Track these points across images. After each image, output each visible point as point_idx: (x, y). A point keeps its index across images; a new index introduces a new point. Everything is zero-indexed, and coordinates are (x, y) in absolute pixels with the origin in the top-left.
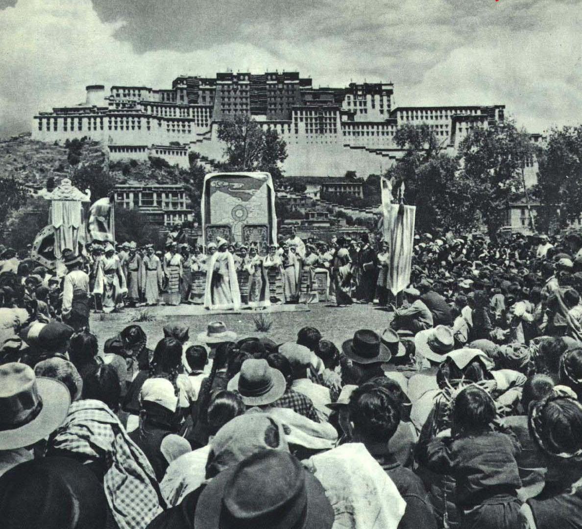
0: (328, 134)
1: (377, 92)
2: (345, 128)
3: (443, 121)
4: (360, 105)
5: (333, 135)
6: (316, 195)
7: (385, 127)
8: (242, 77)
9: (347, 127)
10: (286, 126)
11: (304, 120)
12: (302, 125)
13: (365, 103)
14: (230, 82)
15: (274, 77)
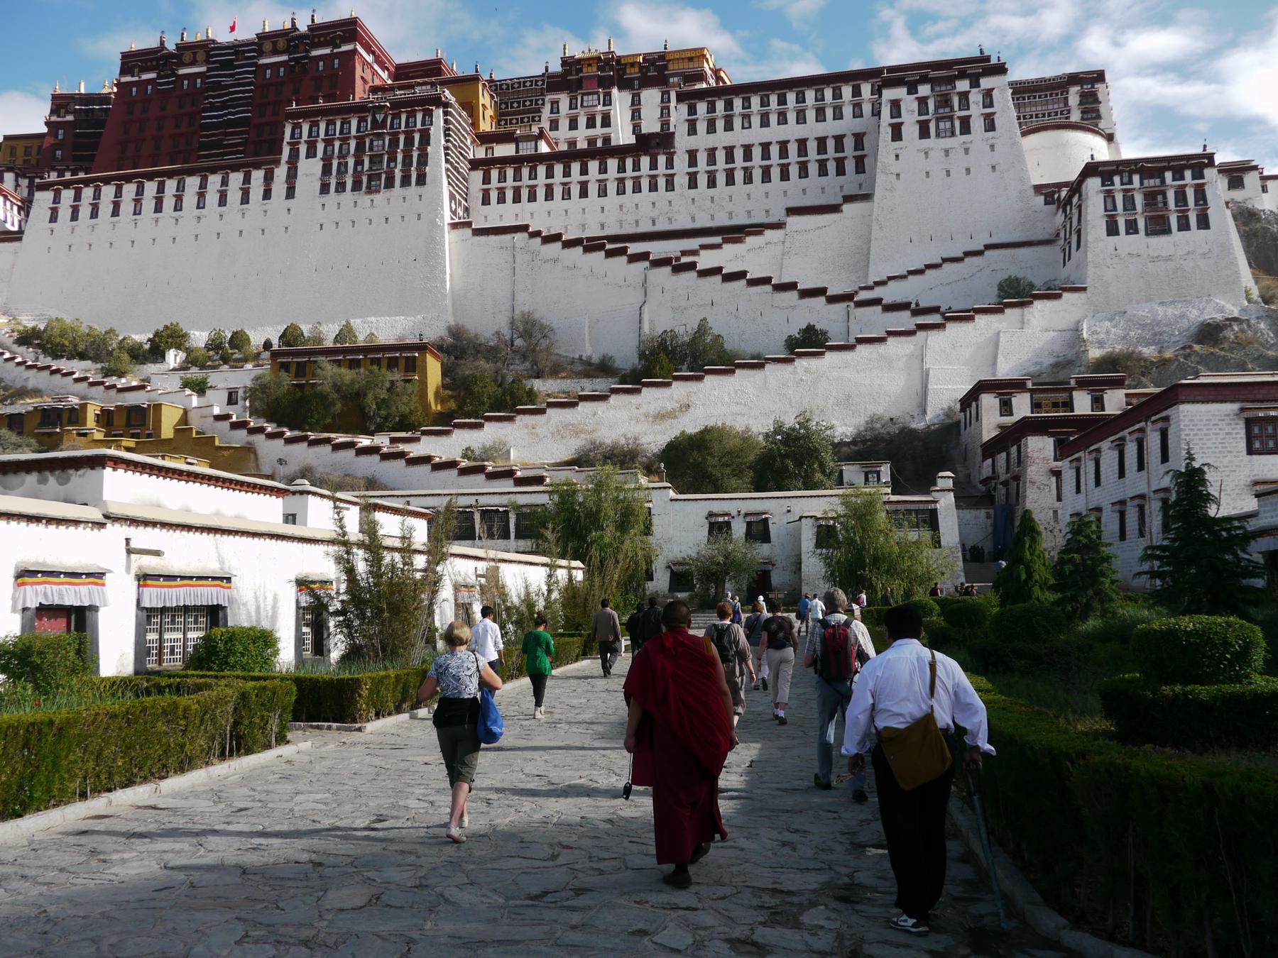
0: (397, 189)
1: (647, 82)
2: (487, 180)
3: (848, 124)
4: (591, 124)
5: (413, 189)
6: (232, 400)
7: (629, 162)
8: (187, 56)
9: (495, 174)
10: (258, 176)
11: (320, 147)
12: (310, 169)
13: (606, 122)
14: (152, 75)
15: (282, 43)
